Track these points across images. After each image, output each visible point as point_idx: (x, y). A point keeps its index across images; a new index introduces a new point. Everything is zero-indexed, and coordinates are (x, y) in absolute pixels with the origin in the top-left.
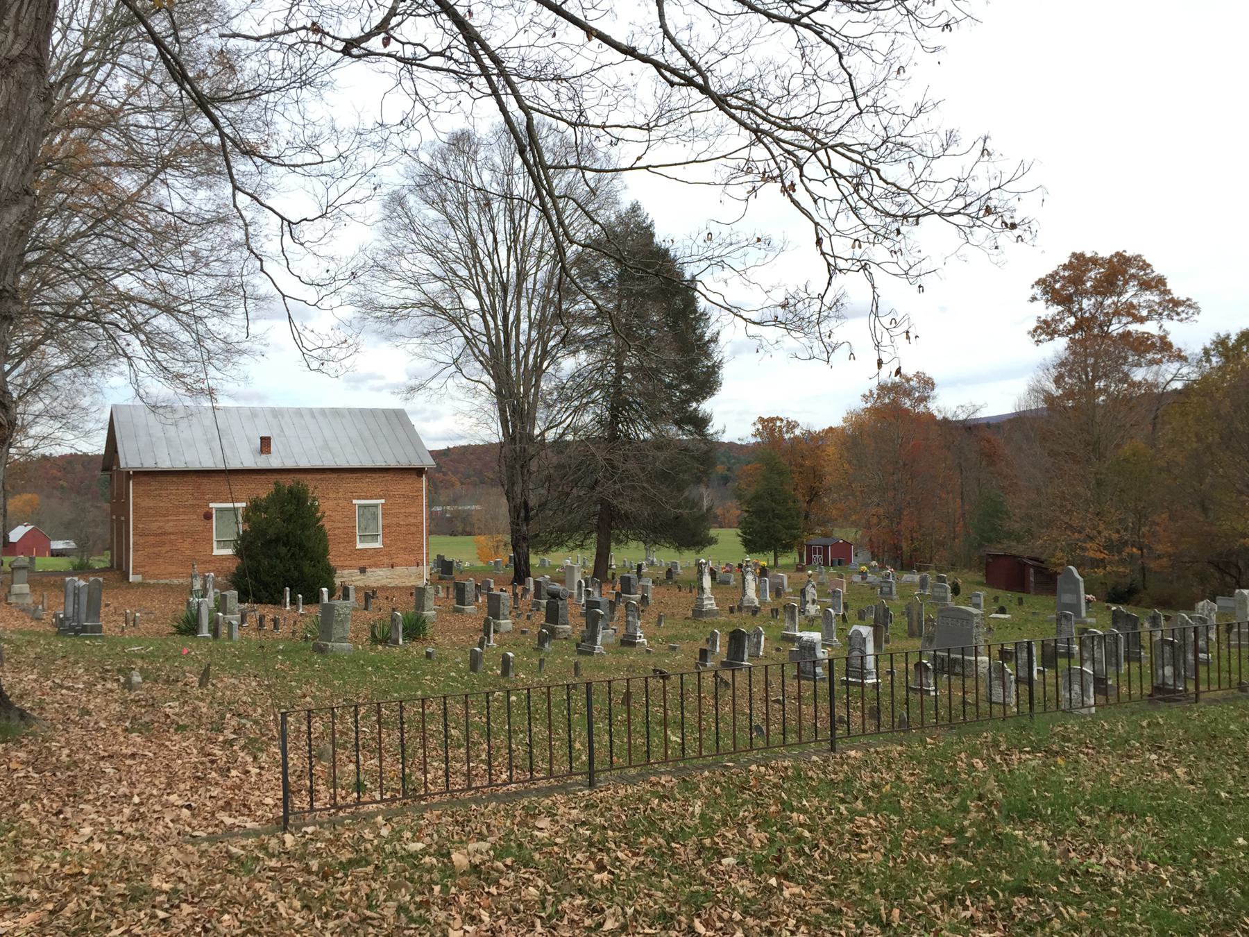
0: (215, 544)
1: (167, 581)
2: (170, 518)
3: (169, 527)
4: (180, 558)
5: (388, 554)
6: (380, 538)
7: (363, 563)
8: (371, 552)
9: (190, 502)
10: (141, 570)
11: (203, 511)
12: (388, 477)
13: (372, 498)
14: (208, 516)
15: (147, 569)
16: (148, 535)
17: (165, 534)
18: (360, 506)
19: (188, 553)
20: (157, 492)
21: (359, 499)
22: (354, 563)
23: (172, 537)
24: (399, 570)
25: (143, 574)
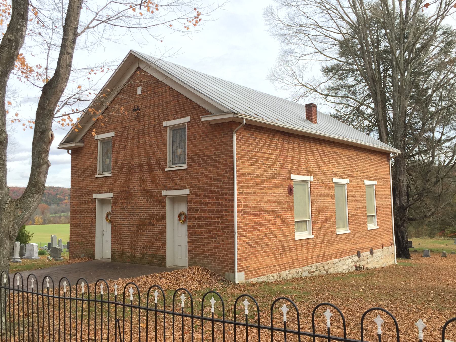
2: (263, 191)
6: (375, 219)
10: (243, 263)
11: (286, 183)
16: (249, 214)
17: (262, 212)
19: (279, 238)
20: (254, 154)
23: (268, 217)
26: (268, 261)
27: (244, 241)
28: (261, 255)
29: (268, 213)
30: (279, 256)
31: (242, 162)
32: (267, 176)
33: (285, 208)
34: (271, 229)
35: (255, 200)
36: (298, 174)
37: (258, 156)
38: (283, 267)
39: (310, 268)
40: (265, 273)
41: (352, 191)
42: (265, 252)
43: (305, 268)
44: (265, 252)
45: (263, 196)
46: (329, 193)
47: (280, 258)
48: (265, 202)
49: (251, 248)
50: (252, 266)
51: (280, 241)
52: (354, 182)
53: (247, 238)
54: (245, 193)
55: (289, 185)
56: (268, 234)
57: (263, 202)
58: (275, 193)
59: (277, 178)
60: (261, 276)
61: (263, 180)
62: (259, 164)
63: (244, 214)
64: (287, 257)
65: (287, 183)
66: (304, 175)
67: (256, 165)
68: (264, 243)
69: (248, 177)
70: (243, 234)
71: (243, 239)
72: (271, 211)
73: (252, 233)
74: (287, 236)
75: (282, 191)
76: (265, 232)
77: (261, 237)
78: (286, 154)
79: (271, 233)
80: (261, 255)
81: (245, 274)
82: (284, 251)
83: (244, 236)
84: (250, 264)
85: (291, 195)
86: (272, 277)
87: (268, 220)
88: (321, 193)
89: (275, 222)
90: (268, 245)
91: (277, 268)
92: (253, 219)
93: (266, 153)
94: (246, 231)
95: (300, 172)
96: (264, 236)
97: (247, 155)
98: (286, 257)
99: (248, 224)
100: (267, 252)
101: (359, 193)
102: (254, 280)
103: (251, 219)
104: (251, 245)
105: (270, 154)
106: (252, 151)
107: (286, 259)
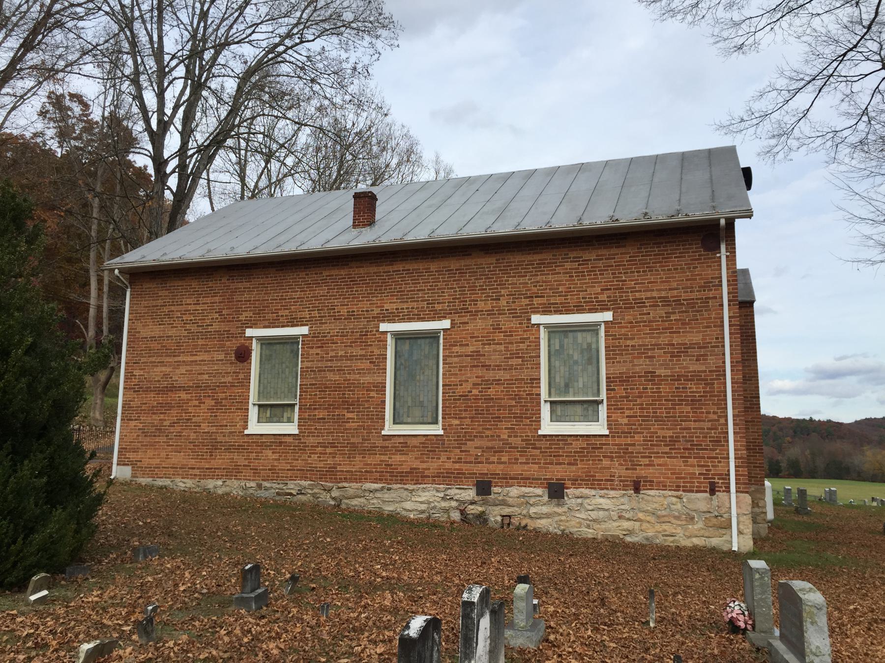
0: (253, 412)
1: (167, 482)
2: (180, 359)
3: (180, 376)
4: (193, 436)
5: (625, 454)
6: (603, 410)
7: (557, 472)
8: (578, 445)
9: (216, 327)
10: (132, 456)
11: (233, 345)
12: (622, 255)
13: (579, 309)
14: (243, 355)
15: (140, 455)
16: (147, 390)
17: (172, 389)
18: (553, 329)
19: (205, 427)
20: (166, 310)
21: (546, 311)
22: (533, 470)
23: (183, 395)
24: (654, 498)
25: (133, 464)
26: (178, 459)
27: (135, 426)
28: (165, 449)
29: (184, 390)
30: (203, 455)
31: (141, 322)
32: (189, 336)
33: (226, 383)
34: (191, 413)
35: (161, 372)
36: (265, 327)
37: (173, 311)
38: (210, 473)
39: (281, 486)
40: (169, 474)
41: (468, 345)
42: (173, 445)
43: (266, 484)
44: (173, 445)
45: (178, 365)
46: (363, 352)
47: (206, 459)
48: (182, 374)
49: (145, 436)
50: (146, 462)
51: (209, 432)
52: (480, 325)
53: (140, 423)
54: (143, 363)
55: (238, 347)
56: (183, 419)
57: (177, 374)
58: (205, 361)
59: (210, 338)
60: (162, 478)
61: (179, 343)
62: (175, 321)
63: (139, 391)
64: (224, 459)
65: (234, 344)
66: (283, 326)
67: (168, 324)
68: (173, 432)
69: (152, 341)
70: (134, 416)
71: (133, 424)
72: (192, 387)
73: (151, 417)
74: (227, 426)
75: (222, 357)
76: (176, 416)
77: (167, 423)
78: (237, 297)
79: (188, 420)
80: (165, 449)
81: (133, 470)
82: (216, 449)
83: (136, 420)
84: (142, 458)
85: (242, 362)
86: (183, 484)
87: (184, 400)
88: (332, 354)
89: (199, 403)
90: (180, 436)
91: (197, 472)
92: (154, 397)
93: (191, 304)
94: (141, 413)
95: (272, 323)
96: (174, 423)
97: (152, 313)
98: (219, 459)
99: (146, 404)
100: (176, 446)
101: (502, 348)
102: (144, 481)
103: (150, 397)
104: (148, 432)
105: (199, 304)
106: (161, 306)
107: (221, 460)
